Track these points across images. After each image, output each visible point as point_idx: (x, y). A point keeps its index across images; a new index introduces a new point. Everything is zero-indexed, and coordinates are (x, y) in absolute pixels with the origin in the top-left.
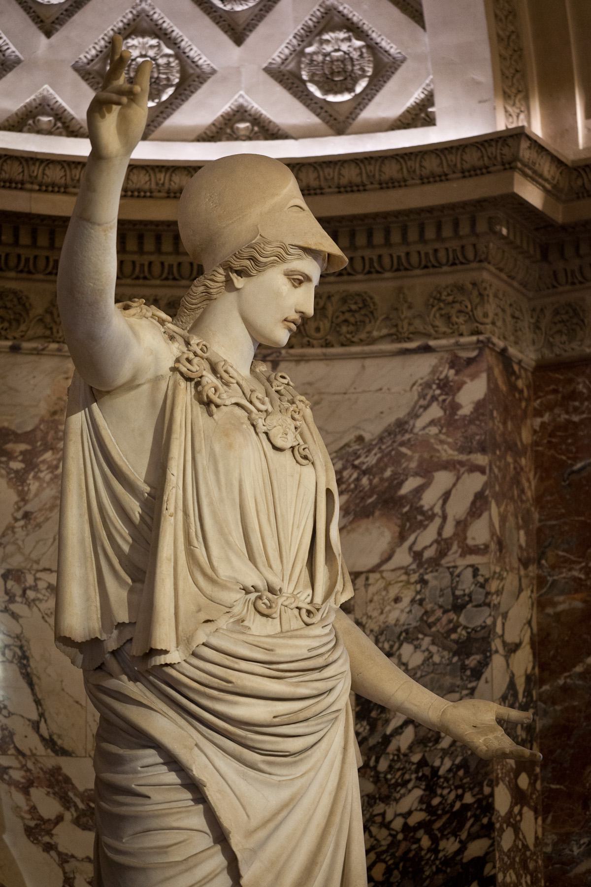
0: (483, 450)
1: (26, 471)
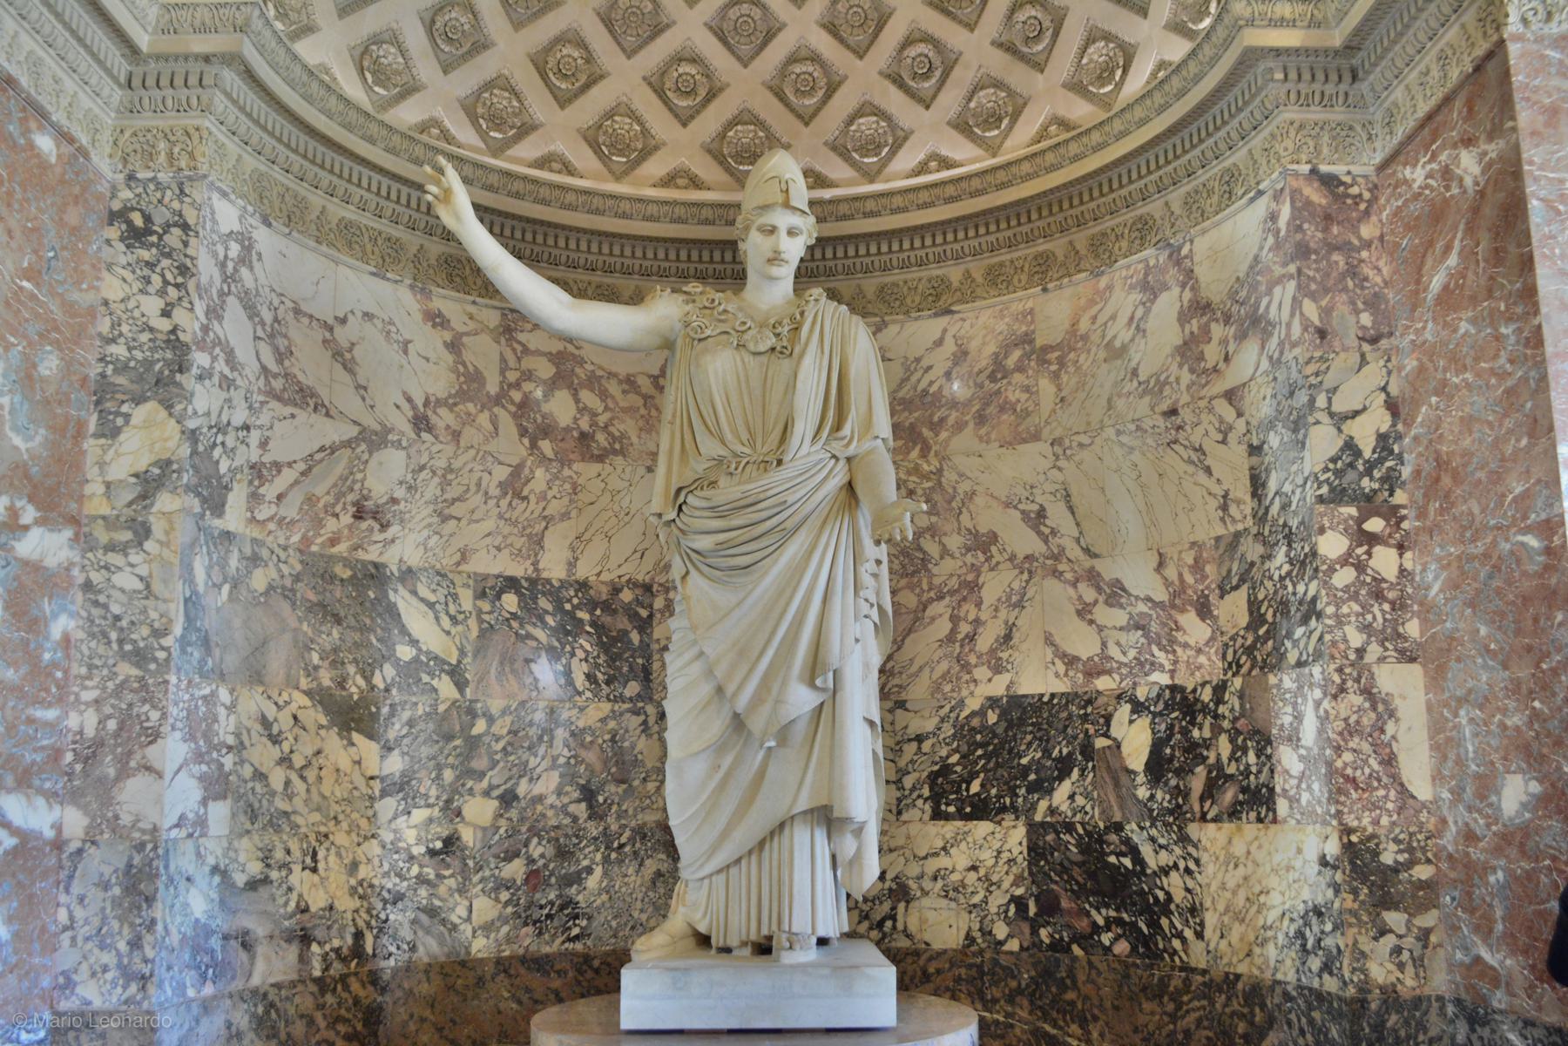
0: (1292, 260)
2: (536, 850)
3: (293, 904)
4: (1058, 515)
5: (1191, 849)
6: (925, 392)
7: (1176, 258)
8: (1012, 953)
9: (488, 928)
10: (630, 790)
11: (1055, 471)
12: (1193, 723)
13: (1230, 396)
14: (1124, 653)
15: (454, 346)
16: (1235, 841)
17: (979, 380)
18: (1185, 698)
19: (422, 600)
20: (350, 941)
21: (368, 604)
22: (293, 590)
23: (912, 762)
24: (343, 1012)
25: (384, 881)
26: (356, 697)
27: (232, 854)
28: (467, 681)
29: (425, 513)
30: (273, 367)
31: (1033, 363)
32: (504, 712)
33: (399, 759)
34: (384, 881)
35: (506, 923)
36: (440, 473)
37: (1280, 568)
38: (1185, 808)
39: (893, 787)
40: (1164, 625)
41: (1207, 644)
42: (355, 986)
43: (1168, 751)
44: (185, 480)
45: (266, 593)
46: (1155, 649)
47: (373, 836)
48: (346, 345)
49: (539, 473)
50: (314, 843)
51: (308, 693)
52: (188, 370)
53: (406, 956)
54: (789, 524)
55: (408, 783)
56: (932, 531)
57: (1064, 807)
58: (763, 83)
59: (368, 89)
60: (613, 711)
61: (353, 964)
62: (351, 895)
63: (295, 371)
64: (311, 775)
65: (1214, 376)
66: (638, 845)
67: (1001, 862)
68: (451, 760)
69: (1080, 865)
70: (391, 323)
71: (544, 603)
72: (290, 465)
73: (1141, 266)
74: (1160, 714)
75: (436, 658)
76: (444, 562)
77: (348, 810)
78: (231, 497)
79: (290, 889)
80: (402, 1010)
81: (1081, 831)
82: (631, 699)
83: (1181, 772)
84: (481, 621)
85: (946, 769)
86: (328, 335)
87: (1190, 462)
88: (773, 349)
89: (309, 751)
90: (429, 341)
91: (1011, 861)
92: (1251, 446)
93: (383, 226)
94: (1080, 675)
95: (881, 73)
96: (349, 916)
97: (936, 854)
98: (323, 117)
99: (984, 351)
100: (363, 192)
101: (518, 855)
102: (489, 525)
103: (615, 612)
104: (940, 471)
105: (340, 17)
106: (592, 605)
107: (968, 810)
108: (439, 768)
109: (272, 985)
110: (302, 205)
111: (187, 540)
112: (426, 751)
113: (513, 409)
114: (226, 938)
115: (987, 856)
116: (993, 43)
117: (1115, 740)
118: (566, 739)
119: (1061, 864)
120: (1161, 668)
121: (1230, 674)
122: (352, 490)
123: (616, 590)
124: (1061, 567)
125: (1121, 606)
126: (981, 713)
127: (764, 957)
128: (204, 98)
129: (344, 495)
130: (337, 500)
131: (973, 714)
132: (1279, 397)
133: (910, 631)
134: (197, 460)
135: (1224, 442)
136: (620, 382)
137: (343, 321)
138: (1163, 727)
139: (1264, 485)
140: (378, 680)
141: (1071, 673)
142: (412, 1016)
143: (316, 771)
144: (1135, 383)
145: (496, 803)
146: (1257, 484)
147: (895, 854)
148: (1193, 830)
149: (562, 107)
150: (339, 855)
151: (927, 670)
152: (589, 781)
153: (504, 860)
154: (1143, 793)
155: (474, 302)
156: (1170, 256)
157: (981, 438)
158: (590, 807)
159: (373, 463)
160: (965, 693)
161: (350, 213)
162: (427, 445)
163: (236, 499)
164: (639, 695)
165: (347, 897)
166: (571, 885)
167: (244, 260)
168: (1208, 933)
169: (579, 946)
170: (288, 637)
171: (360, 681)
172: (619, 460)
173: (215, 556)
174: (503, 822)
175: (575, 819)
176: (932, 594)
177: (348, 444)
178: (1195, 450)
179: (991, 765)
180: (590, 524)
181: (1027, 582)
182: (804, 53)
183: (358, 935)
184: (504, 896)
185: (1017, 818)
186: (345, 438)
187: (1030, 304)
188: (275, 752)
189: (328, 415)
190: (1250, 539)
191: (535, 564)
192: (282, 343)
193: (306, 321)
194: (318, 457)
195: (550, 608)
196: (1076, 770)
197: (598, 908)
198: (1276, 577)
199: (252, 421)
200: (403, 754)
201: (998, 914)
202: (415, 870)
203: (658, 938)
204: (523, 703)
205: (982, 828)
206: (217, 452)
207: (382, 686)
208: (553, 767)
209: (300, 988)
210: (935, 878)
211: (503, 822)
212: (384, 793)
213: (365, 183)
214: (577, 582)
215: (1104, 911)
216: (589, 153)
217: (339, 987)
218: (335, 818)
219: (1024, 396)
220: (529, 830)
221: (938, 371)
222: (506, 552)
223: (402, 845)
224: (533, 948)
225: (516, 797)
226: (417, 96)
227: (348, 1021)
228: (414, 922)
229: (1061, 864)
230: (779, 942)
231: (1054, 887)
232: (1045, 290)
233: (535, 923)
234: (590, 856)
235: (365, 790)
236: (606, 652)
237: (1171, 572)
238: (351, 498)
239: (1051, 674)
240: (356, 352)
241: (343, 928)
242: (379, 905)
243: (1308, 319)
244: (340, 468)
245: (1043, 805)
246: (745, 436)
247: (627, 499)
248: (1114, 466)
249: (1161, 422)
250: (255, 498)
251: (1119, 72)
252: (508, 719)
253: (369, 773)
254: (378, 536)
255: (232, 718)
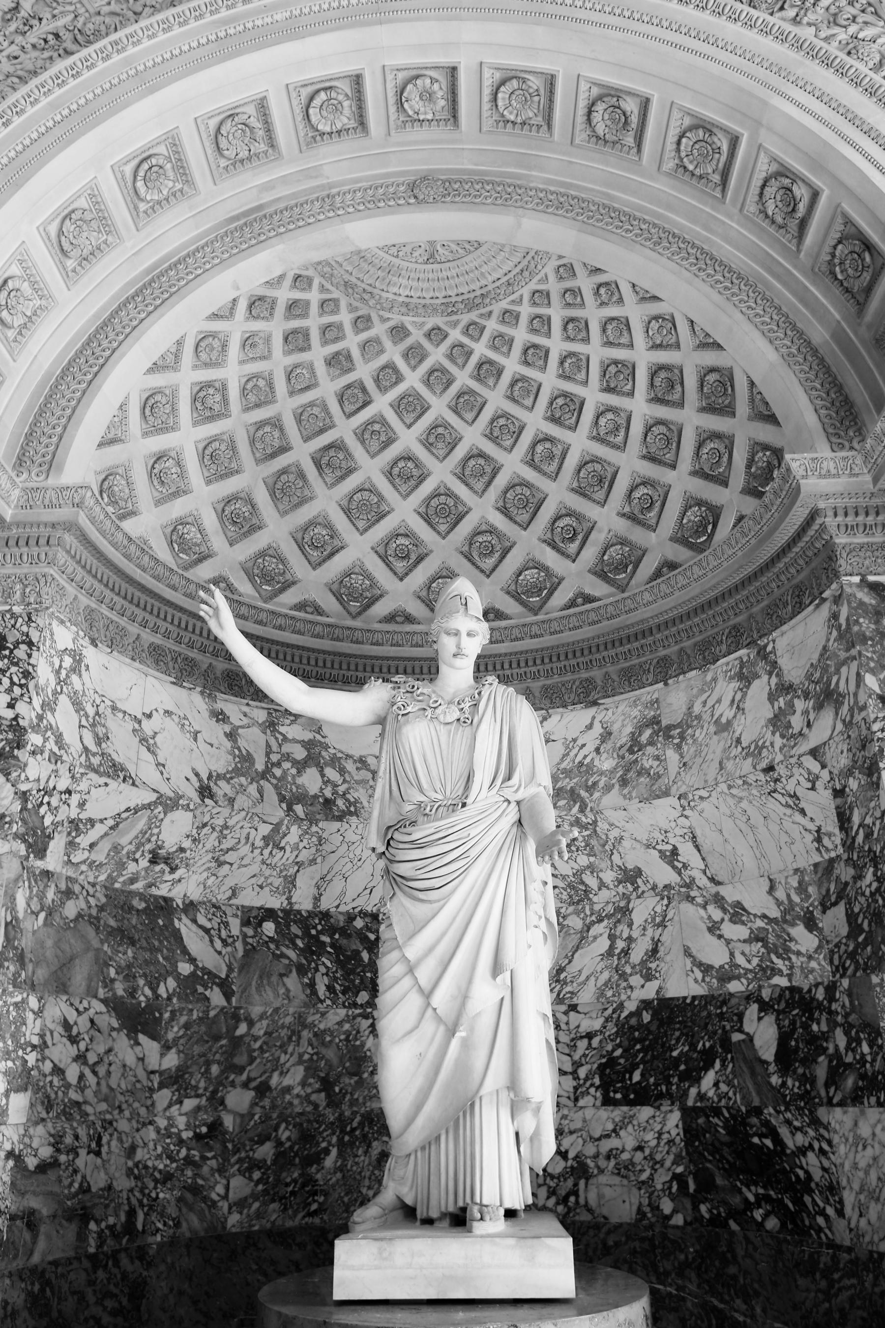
1: (681, 742)
2: (284, 1134)
3: (76, 1185)
4: (687, 852)
5: (822, 1131)
6: (581, 764)
7: (763, 654)
8: (677, 1227)
9: (241, 1204)
10: (360, 1083)
11: (683, 819)
12: (811, 1018)
13: (814, 753)
14: (749, 962)
15: (232, 736)
16: (861, 1124)
17: (621, 753)
18: (802, 998)
19: (201, 927)
20: (123, 1218)
21: (157, 930)
22: (98, 918)
23: (585, 1055)
24: (112, 1287)
25: (157, 1163)
26: (143, 1005)
27: (27, 1140)
28: (233, 993)
29: (204, 860)
30: (93, 748)
31: (660, 739)
32: (262, 1017)
33: (176, 1056)
34: (157, 1163)
35: (256, 1199)
36: (218, 829)
37: (870, 885)
38: (813, 1094)
39: (570, 1077)
40: (778, 937)
41: (816, 951)
42: (124, 1261)
43: (793, 1043)
44: (14, 829)
45: (76, 920)
46: (773, 957)
47: (150, 1123)
48: (150, 733)
49: (294, 829)
50: (99, 1129)
51: (104, 1001)
52: (24, 747)
53: (171, 1231)
54: (473, 853)
55: (182, 1076)
56: (591, 868)
57: (711, 1094)
58: (457, 549)
59: (175, 555)
60: (347, 1016)
61: (124, 1241)
62: (128, 1176)
63: (110, 751)
64: (102, 1070)
65: (800, 739)
66: (366, 1129)
67: (662, 1144)
68: (217, 1057)
69: (729, 1145)
70: (186, 718)
71: (295, 929)
72: (101, 821)
73: (737, 662)
74: (783, 1012)
75: (210, 973)
76: (219, 897)
77: (131, 1100)
78: (52, 845)
79: (75, 1171)
80: (163, 1284)
81: (727, 1115)
82: (362, 1005)
83: (809, 1061)
84: (245, 943)
85: (612, 1062)
86: (137, 726)
87: (787, 806)
88: (458, 720)
89: (101, 1049)
90: (215, 732)
91: (670, 1142)
92: (835, 790)
93: (182, 649)
94: (714, 981)
95: (539, 539)
96: (124, 1195)
97: (608, 1136)
98: (139, 571)
99: (623, 733)
100: (168, 625)
101: (268, 1138)
102: (255, 868)
103: (349, 936)
104: (595, 822)
105: (156, 506)
106: (331, 930)
107: (632, 1096)
108: (208, 1064)
109: (50, 1263)
110: (123, 632)
111: (12, 876)
112: (197, 1049)
113: (274, 781)
114: (13, 1218)
115: (650, 1137)
116: (618, 514)
117: (747, 1034)
118: (309, 1040)
119: (713, 1144)
120: (780, 973)
121: (838, 976)
122: (149, 841)
123: (351, 918)
124: (693, 894)
125: (743, 923)
126: (637, 1013)
127: (460, 1229)
128: (50, 554)
129: (143, 845)
130: (138, 849)
131: (631, 1015)
132: (854, 750)
133: (577, 948)
134: (25, 814)
135: (813, 788)
136: (355, 762)
137: (149, 716)
138: (787, 1022)
139: (849, 820)
140: (162, 991)
141: (707, 979)
142: (171, 1290)
143: (106, 1066)
144: (739, 749)
145: (252, 1093)
146: (843, 819)
147: (575, 1136)
148: (822, 1113)
149: (314, 569)
150: (120, 1140)
151: (593, 979)
152: (328, 1074)
153: (257, 1143)
154: (775, 1080)
155: (248, 704)
156: (758, 653)
157: (624, 796)
158: (328, 1096)
159: (167, 821)
160: (623, 997)
161: (158, 640)
162: (209, 808)
163: (56, 846)
164: (368, 1002)
165: (124, 1177)
166: (311, 1166)
167: (76, 669)
168: (848, 1210)
169: (317, 1220)
170: (91, 955)
171: (148, 992)
172: (354, 820)
173: (35, 890)
174: (258, 1110)
175: (316, 1106)
176: (594, 918)
177: (148, 806)
178: (790, 796)
179: (649, 1057)
180: (332, 868)
181: (667, 906)
182: (484, 527)
183: (131, 1214)
184: (257, 1175)
185: (673, 1104)
186: (146, 802)
187: (656, 696)
188: (73, 1051)
189: (134, 784)
190: (842, 864)
191: (289, 899)
192: (101, 731)
193: (121, 715)
194: (124, 815)
195: (300, 933)
196: (718, 1062)
197: (333, 1186)
198: (867, 893)
199: (73, 787)
200: (179, 1052)
201: (663, 1190)
202: (184, 1152)
203: (372, 1211)
204: (276, 1010)
205: (645, 1112)
206: (43, 810)
207: (165, 996)
208: (300, 1062)
209: (76, 1264)
210: (608, 1157)
211: (258, 1110)
212: (162, 1086)
213: (169, 619)
214: (321, 912)
215: (753, 1188)
216: (334, 600)
217: (110, 1263)
218: (119, 1107)
219: (657, 763)
220: (278, 1117)
221: (590, 747)
222: (267, 889)
223: (174, 1130)
224: (279, 1222)
225: (269, 1088)
226: (210, 560)
227: (116, 1296)
228: (180, 1200)
229: (713, 1144)
230: (472, 1215)
231: (708, 1165)
232: (666, 684)
233: (281, 1199)
234: (329, 1140)
235: (145, 1082)
236: (343, 968)
237: (780, 894)
238: (148, 847)
239: (691, 980)
240: (158, 739)
241: (120, 1205)
242: (151, 1185)
243: (870, 689)
244: (141, 823)
245: (693, 1091)
246: (438, 786)
247: (360, 848)
248: (728, 813)
249: (761, 777)
250: (72, 845)
251: (710, 527)
252: (265, 1023)
253: (150, 1068)
254: (168, 877)
255: (39, 1022)
